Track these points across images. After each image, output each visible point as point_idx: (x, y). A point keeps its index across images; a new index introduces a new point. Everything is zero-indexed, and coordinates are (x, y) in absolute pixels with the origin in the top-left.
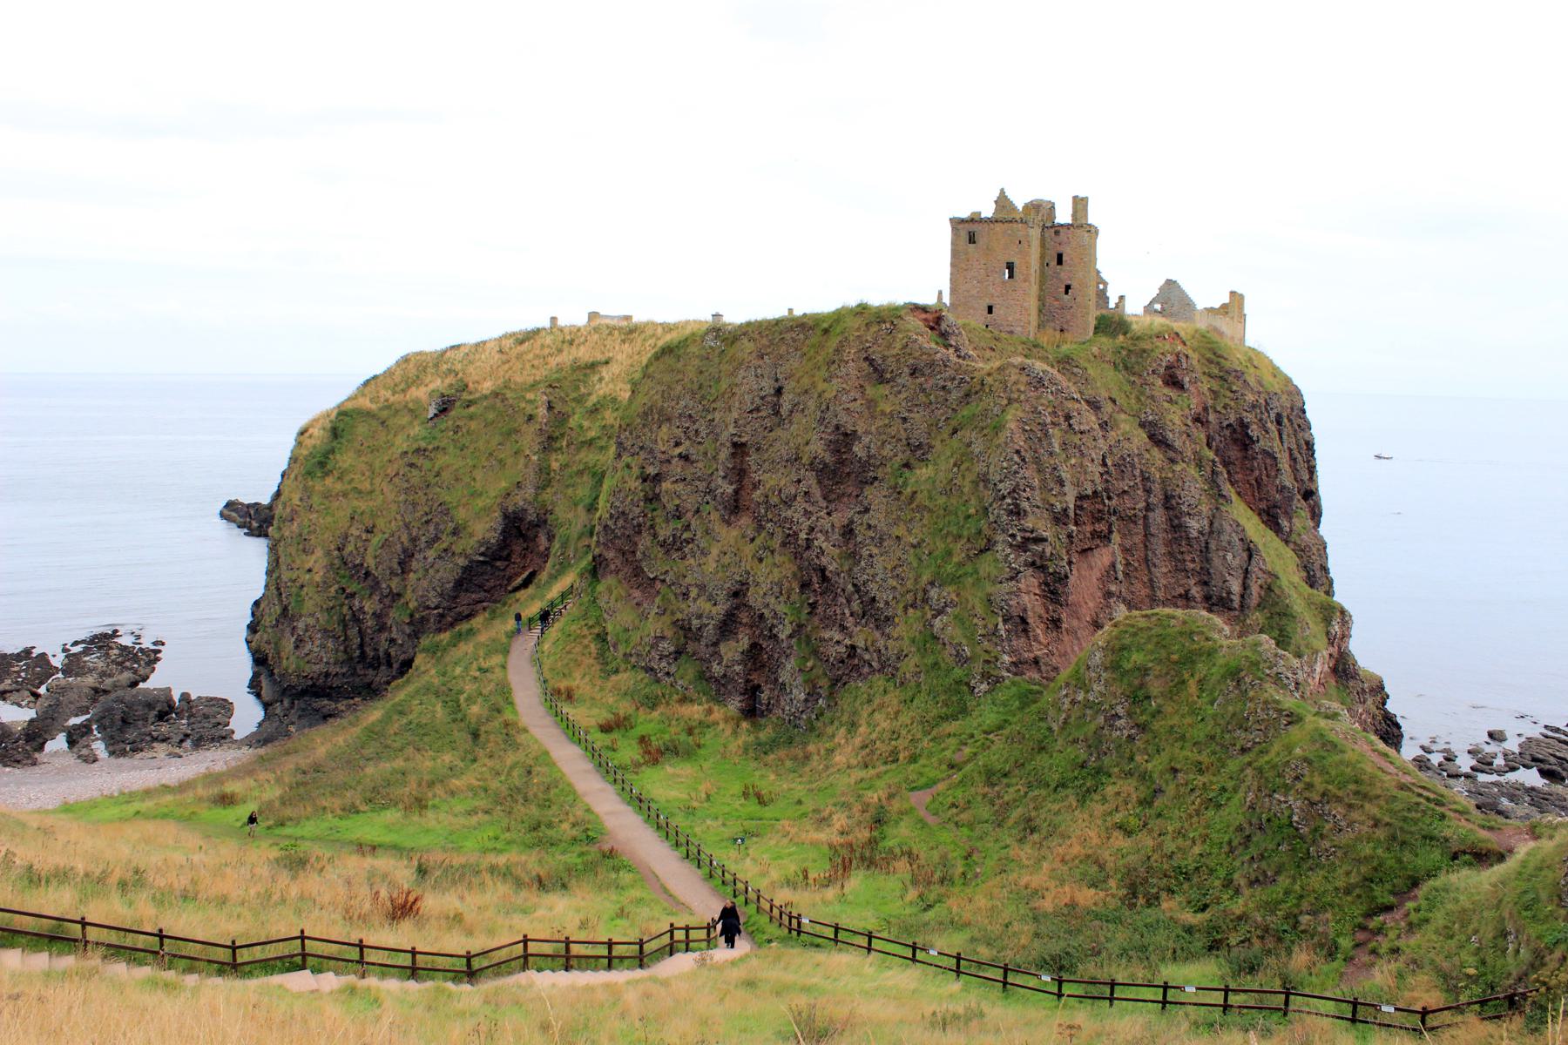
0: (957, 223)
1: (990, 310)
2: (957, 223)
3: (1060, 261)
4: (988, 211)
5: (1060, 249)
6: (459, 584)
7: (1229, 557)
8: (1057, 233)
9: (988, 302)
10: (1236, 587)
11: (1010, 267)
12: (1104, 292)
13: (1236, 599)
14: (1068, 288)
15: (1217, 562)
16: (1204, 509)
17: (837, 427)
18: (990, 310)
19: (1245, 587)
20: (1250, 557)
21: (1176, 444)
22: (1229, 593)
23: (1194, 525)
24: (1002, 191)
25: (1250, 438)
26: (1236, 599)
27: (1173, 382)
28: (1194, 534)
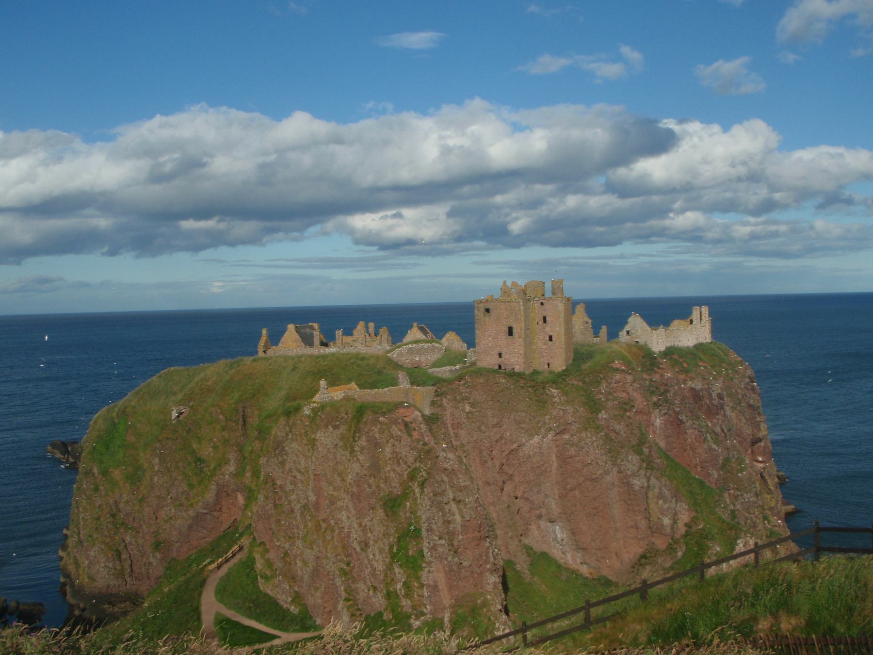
1: (500, 355)
4: (497, 295)
5: (545, 314)
6: (190, 527)
9: (497, 350)
10: (667, 521)
14: (551, 338)
15: (652, 506)
16: (642, 472)
17: (357, 474)
18: (500, 355)
19: (675, 521)
21: (622, 433)
23: (637, 483)
24: (505, 282)
28: (637, 488)
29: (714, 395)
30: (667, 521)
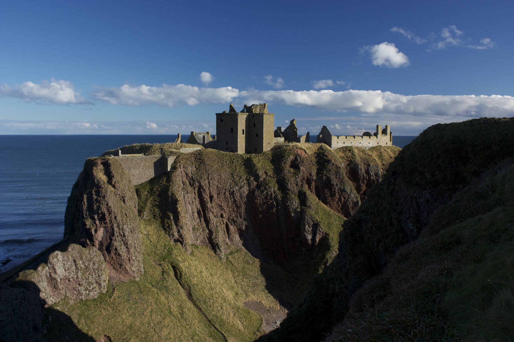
0: (218, 115)
1: (227, 143)
2: (218, 115)
3: (255, 126)
4: (227, 111)
7: (307, 227)
8: (253, 116)
10: (309, 237)
11: (232, 129)
12: (296, 132)
13: (310, 242)
18: (227, 143)
20: (317, 227)
22: (307, 240)
25: (333, 185)
26: (310, 242)
27: (295, 165)
29: (372, 173)
30: (309, 237)
